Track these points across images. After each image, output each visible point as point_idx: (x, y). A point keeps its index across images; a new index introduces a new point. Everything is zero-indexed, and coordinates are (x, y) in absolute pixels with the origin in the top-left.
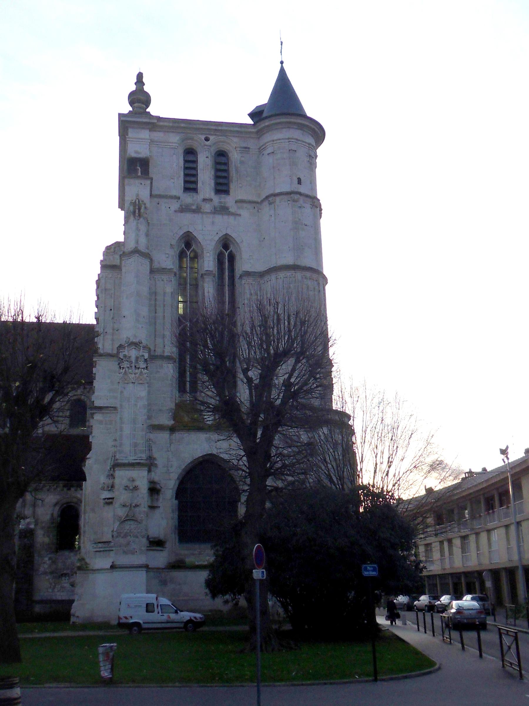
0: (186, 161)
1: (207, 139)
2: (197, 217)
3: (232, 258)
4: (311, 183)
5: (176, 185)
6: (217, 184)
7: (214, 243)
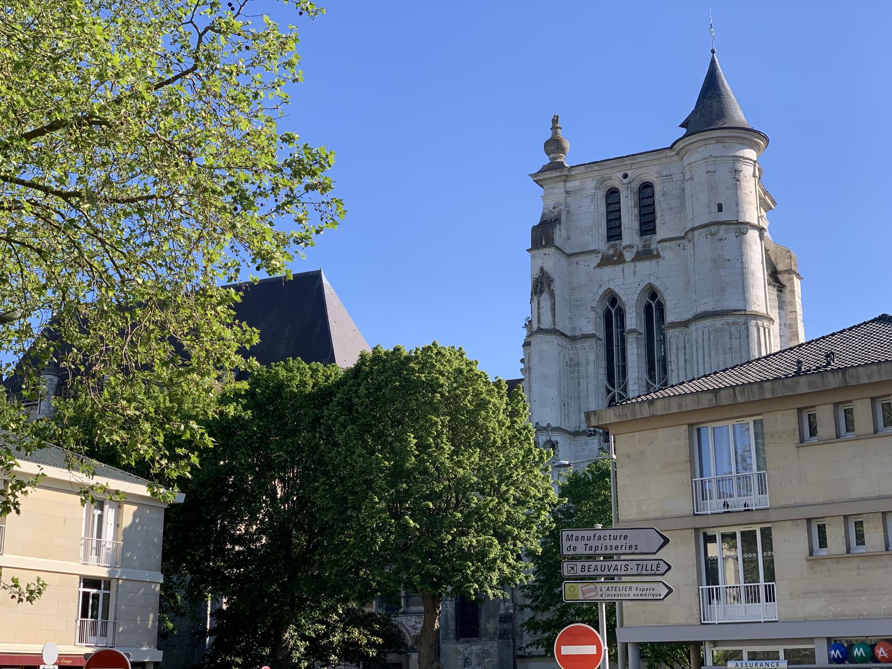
0: (608, 205)
1: (625, 176)
2: (618, 268)
3: (661, 308)
4: (737, 205)
5: (597, 239)
6: (642, 224)
7: (636, 296)
